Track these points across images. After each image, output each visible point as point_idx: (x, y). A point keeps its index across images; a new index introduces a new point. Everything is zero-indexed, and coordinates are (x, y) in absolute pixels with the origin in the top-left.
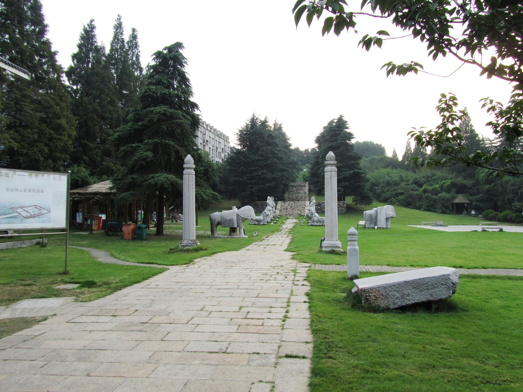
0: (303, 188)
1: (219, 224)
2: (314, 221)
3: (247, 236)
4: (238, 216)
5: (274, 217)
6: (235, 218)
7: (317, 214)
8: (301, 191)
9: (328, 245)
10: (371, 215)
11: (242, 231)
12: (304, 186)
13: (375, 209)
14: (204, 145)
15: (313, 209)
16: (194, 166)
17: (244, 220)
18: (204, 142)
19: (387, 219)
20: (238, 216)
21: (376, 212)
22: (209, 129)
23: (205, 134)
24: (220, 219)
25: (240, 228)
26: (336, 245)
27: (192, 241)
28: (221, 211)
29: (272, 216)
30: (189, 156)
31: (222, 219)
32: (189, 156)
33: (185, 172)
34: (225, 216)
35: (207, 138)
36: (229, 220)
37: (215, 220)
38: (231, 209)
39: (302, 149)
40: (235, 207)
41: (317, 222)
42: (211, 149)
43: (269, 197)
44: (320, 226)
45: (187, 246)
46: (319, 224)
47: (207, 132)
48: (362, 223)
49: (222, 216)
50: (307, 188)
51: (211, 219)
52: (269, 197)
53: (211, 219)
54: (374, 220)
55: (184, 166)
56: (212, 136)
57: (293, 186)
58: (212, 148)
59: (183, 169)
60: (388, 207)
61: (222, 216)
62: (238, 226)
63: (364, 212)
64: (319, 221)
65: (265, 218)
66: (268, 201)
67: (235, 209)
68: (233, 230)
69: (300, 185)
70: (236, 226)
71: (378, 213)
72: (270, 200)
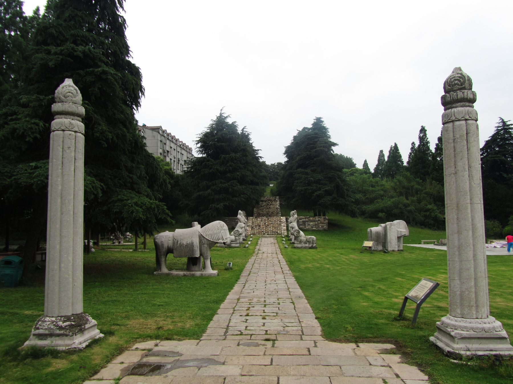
0: (274, 203)
1: (170, 250)
2: (301, 242)
3: (215, 272)
4: (201, 237)
5: (246, 236)
6: (196, 241)
7: (302, 233)
8: (272, 206)
9: (471, 333)
10: (377, 233)
11: (208, 263)
12: (275, 200)
13: (383, 225)
14: (165, 156)
15: (295, 225)
16: (82, 110)
17: (212, 244)
18: (164, 152)
19: (399, 238)
20: (201, 237)
21: (385, 229)
22: (170, 138)
23: (165, 144)
24: (170, 243)
25: (205, 259)
26: (495, 334)
27: (68, 318)
28: (174, 231)
29: (244, 235)
30: (69, 82)
31: (174, 243)
32: (69, 82)
33: (57, 122)
35: (168, 148)
36: (187, 245)
37: (163, 245)
38: (190, 226)
39: (269, 163)
40: (196, 223)
41: (305, 243)
42: (172, 161)
43: (240, 211)
44: (310, 248)
45: (51, 335)
46: (307, 245)
47: (168, 142)
48: (368, 244)
49: (174, 239)
50: (278, 203)
51: (156, 244)
52: (240, 211)
53: (156, 244)
54: (382, 240)
55: (56, 107)
56: (172, 145)
57: (262, 201)
58: (173, 159)
59: (50, 116)
60: (399, 223)
61: (174, 239)
62: (201, 254)
63: (369, 230)
64: (307, 241)
65: (237, 238)
66: (239, 216)
67: (197, 227)
68: (193, 262)
69: (269, 200)
70: (197, 255)
71: (388, 230)
72: (241, 215)
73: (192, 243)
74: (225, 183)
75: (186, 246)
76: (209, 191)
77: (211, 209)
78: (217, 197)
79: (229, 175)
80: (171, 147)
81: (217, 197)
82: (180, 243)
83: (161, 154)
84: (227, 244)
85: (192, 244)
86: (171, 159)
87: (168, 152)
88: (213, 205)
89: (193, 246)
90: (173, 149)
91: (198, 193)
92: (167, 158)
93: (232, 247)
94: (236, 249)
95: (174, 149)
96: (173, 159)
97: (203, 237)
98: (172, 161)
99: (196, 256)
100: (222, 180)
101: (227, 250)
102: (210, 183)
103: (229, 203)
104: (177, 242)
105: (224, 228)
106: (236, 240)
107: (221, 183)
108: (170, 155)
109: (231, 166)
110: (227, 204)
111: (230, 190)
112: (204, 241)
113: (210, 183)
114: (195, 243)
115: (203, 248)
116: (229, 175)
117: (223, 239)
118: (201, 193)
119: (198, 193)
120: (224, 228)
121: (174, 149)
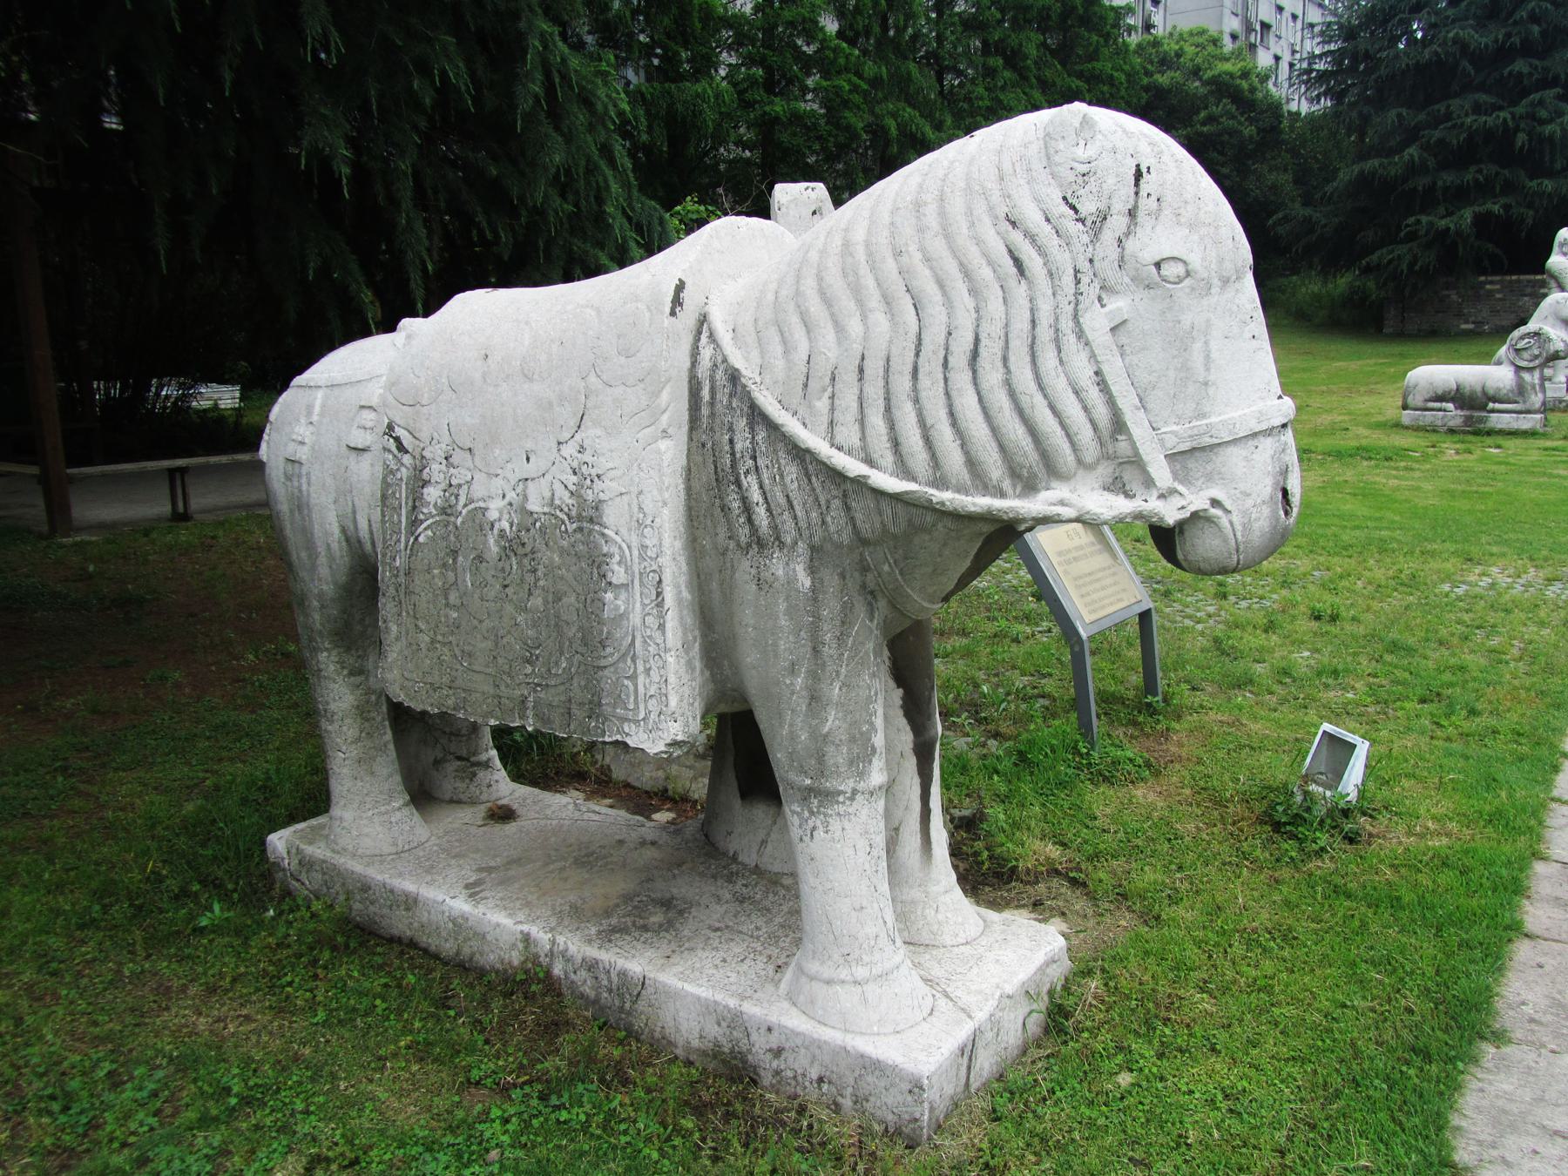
4: (723, 421)
6: (644, 493)
14: (1252, 47)
18: (1249, 29)
20: (723, 421)
34: (431, 430)
42: (1284, 66)
65: (1531, 378)
73: (588, 516)
74: (1501, 108)
75: (512, 546)
76: (1413, 151)
77: (1412, 236)
78: (1448, 178)
79: (1520, 66)
80: (1280, 9)
81: (1448, 178)
82: (446, 510)
83: (1234, 37)
84: (1204, 546)
85: (564, 551)
86: (1277, 58)
87: (1265, 27)
88: (1424, 219)
89: (596, 563)
90: (1287, 14)
91: (1356, 168)
92: (1261, 52)
93: (1490, 433)
94: (1512, 444)
95: (1294, 17)
96: (1286, 58)
97: (757, 416)
98: (1284, 66)
99: (637, 738)
100: (1483, 98)
101: (1450, 450)
102: (1422, 116)
103: (1507, 207)
104: (419, 482)
105: (1152, 242)
106: (1521, 390)
107: (1478, 109)
108: (1272, 39)
109: (1534, 18)
110: (1496, 208)
111: (1521, 138)
112: (766, 487)
113: (1422, 116)
114: (615, 517)
115: (747, 618)
116: (1520, 66)
117: (1126, 470)
118: (1373, 163)
119: (1356, 168)
120: (1152, 242)
121: (1294, 17)
